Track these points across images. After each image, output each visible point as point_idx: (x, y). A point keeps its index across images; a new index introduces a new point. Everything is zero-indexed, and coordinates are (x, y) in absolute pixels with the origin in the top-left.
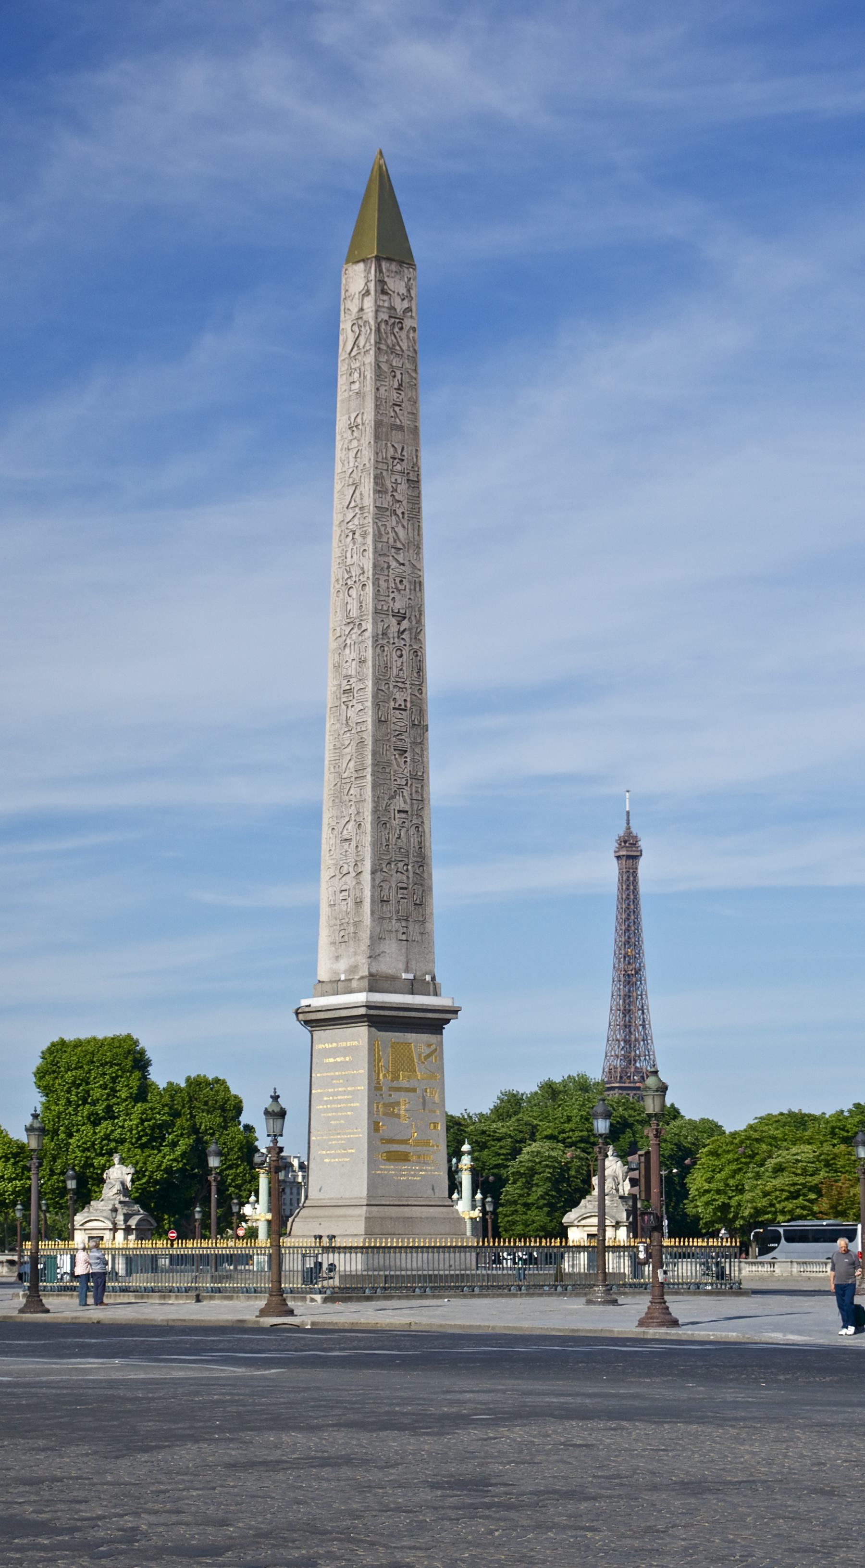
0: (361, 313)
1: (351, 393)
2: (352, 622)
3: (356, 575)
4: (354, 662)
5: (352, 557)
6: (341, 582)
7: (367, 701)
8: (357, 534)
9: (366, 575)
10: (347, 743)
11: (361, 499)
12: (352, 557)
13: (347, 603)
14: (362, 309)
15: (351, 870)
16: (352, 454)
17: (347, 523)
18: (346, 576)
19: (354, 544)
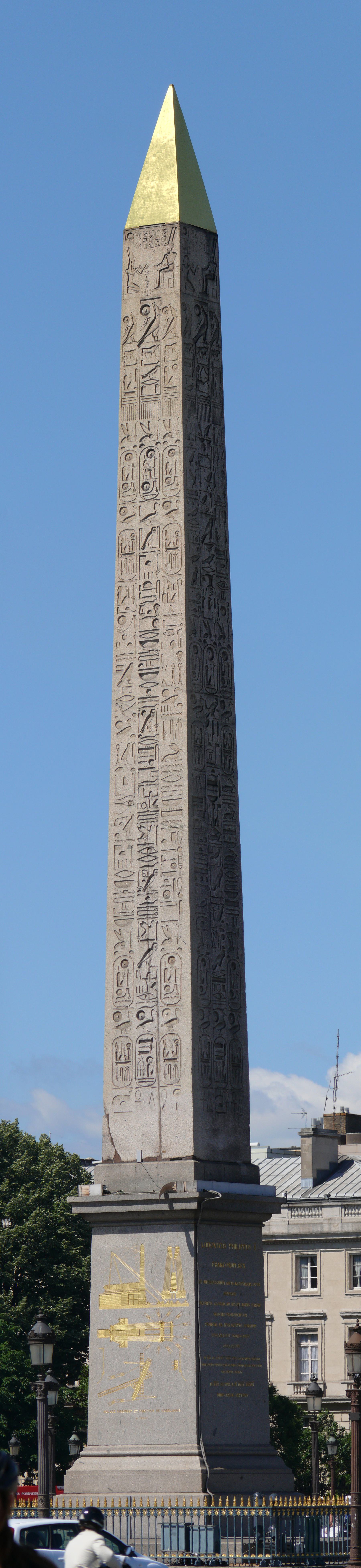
0: (205, 297)
1: (199, 394)
2: (213, 695)
3: (215, 636)
4: (218, 749)
5: (209, 608)
6: (198, 634)
7: (235, 805)
8: (214, 582)
9: (226, 640)
10: (215, 851)
11: (217, 539)
12: (209, 608)
13: (207, 666)
14: (205, 293)
15: (226, 1019)
16: (204, 475)
17: (204, 561)
18: (205, 631)
19: (212, 593)
